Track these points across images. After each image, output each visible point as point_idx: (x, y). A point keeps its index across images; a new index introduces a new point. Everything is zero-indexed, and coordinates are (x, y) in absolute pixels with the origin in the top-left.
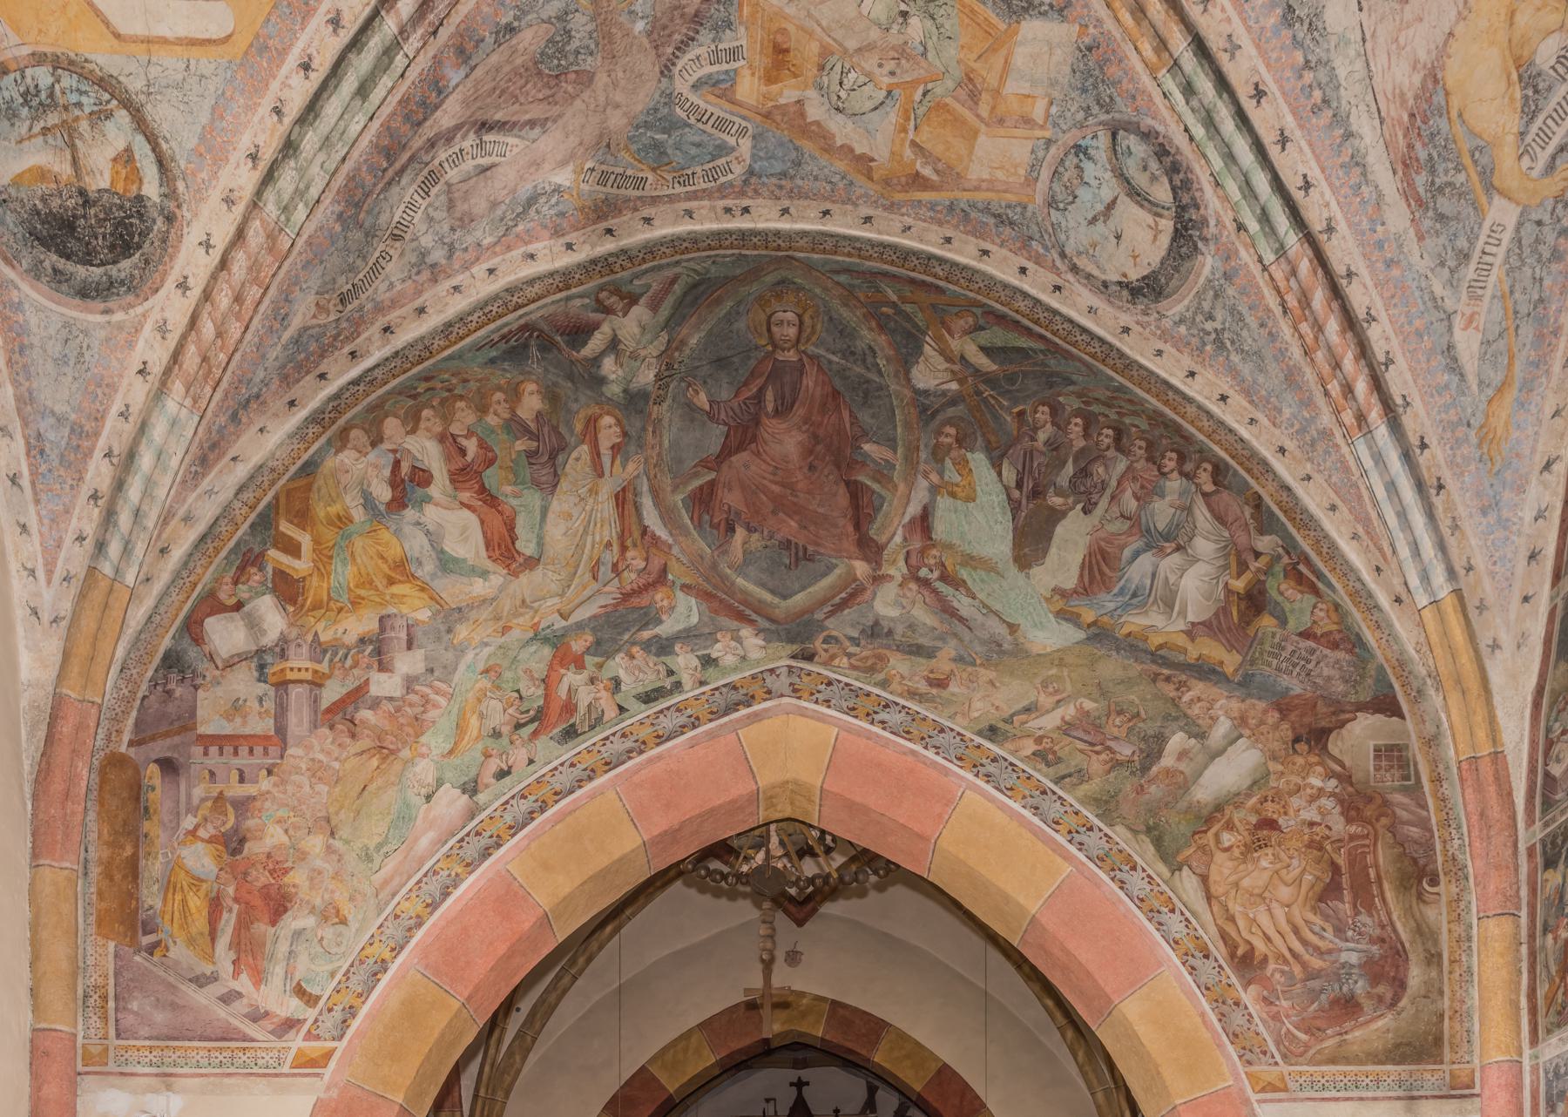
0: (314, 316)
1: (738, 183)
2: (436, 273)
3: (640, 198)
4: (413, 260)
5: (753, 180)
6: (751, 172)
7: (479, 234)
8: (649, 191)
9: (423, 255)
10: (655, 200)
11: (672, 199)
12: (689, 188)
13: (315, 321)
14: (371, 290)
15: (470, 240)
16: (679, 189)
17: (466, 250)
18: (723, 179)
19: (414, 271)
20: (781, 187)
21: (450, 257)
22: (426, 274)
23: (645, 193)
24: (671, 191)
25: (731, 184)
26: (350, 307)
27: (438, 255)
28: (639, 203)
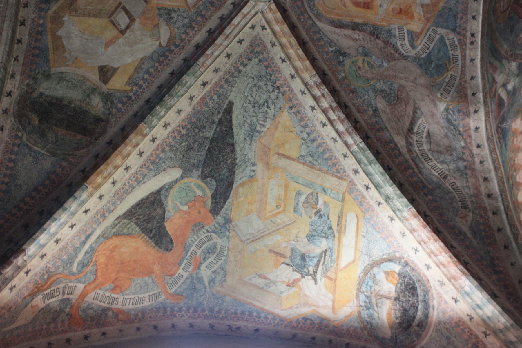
0: (467, 221)
1: (459, 36)
2: (471, 167)
3: (460, 79)
4: (459, 174)
5: (458, 30)
6: (454, 30)
7: (458, 146)
8: (458, 75)
9: (458, 169)
10: (463, 73)
11: (464, 66)
12: (460, 58)
13: (469, 222)
14: (466, 196)
15: (459, 150)
16: (460, 62)
17: (463, 153)
18: (457, 43)
19: (465, 176)
20: (462, 18)
21: (464, 160)
22: (469, 172)
23: (459, 76)
24: (460, 66)
25: (459, 41)
26: (470, 206)
27: (461, 164)
28: (463, 80)
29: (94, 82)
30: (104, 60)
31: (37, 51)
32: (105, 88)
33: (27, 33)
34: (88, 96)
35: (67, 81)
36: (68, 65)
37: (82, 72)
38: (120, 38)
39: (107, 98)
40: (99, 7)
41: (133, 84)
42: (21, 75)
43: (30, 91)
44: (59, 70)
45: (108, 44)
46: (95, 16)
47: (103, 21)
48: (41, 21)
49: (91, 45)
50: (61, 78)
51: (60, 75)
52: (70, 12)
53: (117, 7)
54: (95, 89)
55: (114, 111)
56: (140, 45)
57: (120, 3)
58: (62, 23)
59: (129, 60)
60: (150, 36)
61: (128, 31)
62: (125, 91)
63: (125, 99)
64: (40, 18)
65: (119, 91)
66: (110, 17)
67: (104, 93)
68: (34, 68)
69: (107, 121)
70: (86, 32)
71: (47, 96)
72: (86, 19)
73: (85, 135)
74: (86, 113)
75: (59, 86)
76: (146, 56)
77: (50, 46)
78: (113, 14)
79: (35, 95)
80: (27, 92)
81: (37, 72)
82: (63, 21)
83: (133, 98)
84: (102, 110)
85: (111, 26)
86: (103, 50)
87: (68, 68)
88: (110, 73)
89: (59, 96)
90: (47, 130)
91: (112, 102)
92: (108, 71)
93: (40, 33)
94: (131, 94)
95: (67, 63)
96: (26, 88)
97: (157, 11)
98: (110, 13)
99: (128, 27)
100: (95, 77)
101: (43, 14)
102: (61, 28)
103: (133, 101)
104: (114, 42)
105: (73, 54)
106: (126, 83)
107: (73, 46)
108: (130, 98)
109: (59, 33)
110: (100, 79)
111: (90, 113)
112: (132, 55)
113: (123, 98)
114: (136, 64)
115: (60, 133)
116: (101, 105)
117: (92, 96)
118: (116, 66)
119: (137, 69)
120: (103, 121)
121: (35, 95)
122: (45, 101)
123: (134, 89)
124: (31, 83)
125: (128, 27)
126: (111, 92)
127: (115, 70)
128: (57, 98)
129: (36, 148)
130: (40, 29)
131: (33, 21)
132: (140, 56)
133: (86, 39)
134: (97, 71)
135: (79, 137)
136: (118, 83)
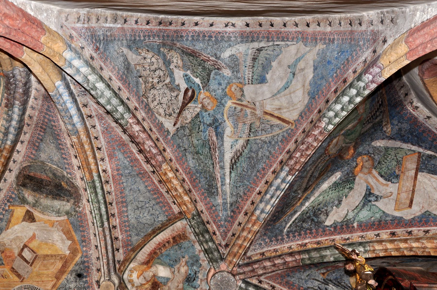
29: (36, 211)
30: (33, 226)
31: (81, 229)
32: (27, 207)
33: (92, 241)
34: (37, 202)
35: (53, 211)
36: (57, 221)
37: (46, 217)
38: (27, 241)
39: (24, 201)
40: (45, 262)
41: (9, 211)
42: (86, 213)
43: (76, 203)
44: (62, 218)
45: (33, 237)
46: (47, 256)
47: (41, 252)
48: (84, 249)
49: (45, 236)
50: (58, 213)
51: (60, 215)
52: (65, 257)
53: (33, 263)
54: (34, 206)
55: (16, 192)
56: (11, 238)
57: (31, 266)
58: (69, 249)
59: (16, 227)
60: (5, 245)
61: (22, 247)
62: (13, 206)
63: (11, 200)
64: (86, 251)
65: (17, 206)
66: (37, 256)
67: (27, 204)
68: (79, 218)
69: (17, 185)
70: (51, 244)
71: (64, 200)
72: (53, 253)
73: (28, 175)
74: (34, 191)
75: (58, 208)
76: (6, 230)
77: (73, 233)
78: (35, 258)
79: (72, 201)
80: (78, 203)
81: (76, 216)
82: (70, 250)
83: (6, 201)
84: (24, 192)
85: (35, 249)
86: (36, 233)
87: (56, 220)
88: (27, 217)
89: (56, 201)
90: (54, 178)
91: (19, 198)
92: (29, 219)
93: (83, 241)
94: (9, 204)
95: (58, 223)
96: (80, 205)
97: (4, 263)
98: (37, 259)
99: (22, 250)
100: (36, 214)
101: (85, 254)
102: (70, 246)
103: (6, 199)
104: (30, 239)
105: (56, 229)
106: (14, 211)
107: (57, 234)
108: (8, 201)
109: (70, 242)
110: (32, 213)
111: (31, 190)
112: (15, 231)
113: (13, 201)
114: (11, 225)
115: (45, 176)
116: (26, 196)
117: (34, 202)
118: (24, 223)
119: (9, 221)
120: (21, 185)
121: (72, 201)
122: (64, 197)
123: (7, 208)
124: (78, 208)
125: (22, 250)
126: (22, 205)
127: (24, 220)
128: (57, 199)
129: (56, 167)
130: (84, 244)
131: (90, 249)
132: (9, 230)
133: (50, 240)
134: (36, 219)
135: (32, 174)
136: (20, 211)
